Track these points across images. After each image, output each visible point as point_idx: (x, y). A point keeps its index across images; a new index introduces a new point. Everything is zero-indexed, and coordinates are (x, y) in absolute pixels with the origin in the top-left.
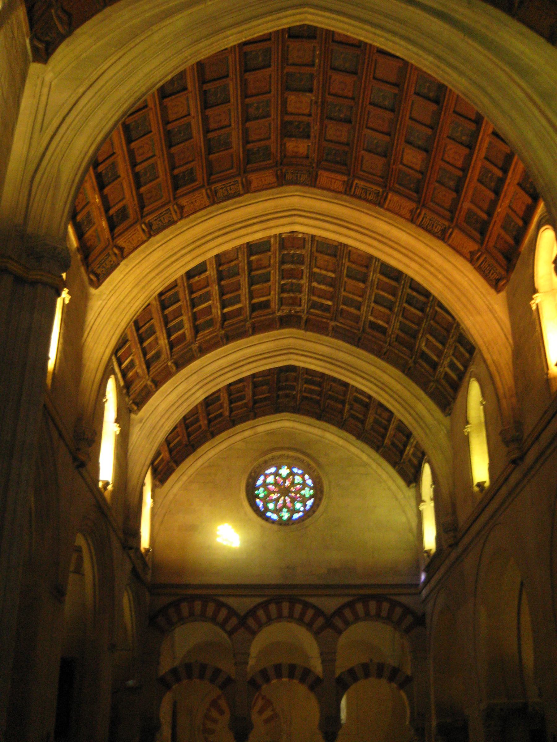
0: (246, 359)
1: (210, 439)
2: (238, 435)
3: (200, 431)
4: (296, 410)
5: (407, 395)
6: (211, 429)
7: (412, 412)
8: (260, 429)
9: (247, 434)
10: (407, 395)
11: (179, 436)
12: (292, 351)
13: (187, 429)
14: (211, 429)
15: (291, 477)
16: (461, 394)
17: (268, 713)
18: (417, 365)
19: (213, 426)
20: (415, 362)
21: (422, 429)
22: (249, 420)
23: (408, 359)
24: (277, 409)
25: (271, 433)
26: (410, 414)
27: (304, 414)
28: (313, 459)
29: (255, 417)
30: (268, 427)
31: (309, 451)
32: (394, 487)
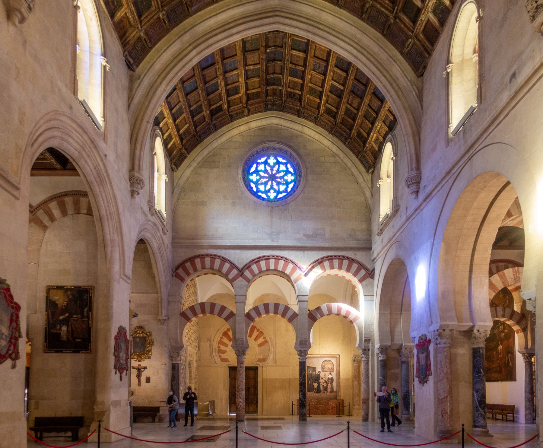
0: (235, 21)
1: (213, 132)
2: (235, 129)
3: (205, 123)
4: (282, 108)
5: (383, 56)
6: (214, 122)
7: (387, 75)
8: (254, 125)
9: (243, 128)
10: (383, 56)
11: (186, 124)
12: (278, 13)
13: (193, 117)
14: (214, 122)
15: (277, 166)
16: (440, 46)
17: (261, 340)
18: (397, 20)
19: (215, 120)
20: (395, 18)
21: (395, 91)
22: (244, 116)
23: (389, 14)
24: (266, 109)
25: (261, 129)
26: (385, 77)
27: (287, 112)
28: (295, 150)
29: (249, 113)
30: (259, 123)
31: (291, 144)
32: (356, 172)
